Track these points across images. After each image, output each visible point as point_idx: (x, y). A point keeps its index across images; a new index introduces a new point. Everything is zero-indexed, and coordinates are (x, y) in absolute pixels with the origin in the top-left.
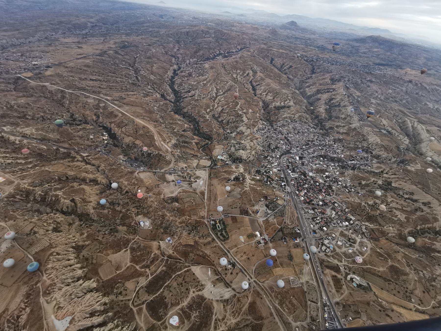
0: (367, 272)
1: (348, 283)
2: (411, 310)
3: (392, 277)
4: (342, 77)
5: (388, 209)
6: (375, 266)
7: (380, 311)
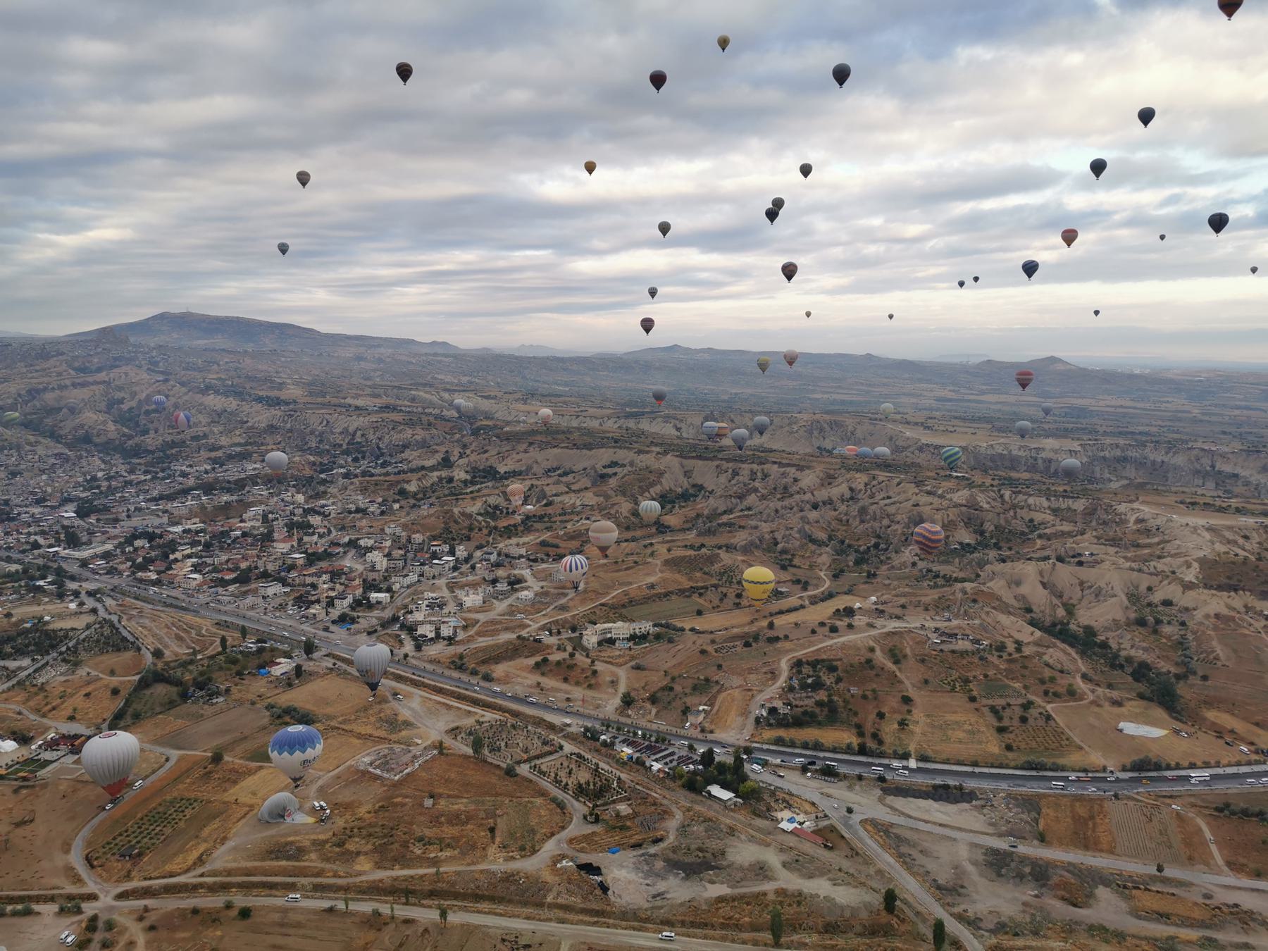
0: (624, 606)
1: (603, 654)
2: (802, 607)
3: (690, 579)
4: (116, 359)
5: (538, 501)
6: (631, 583)
7: (747, 645)
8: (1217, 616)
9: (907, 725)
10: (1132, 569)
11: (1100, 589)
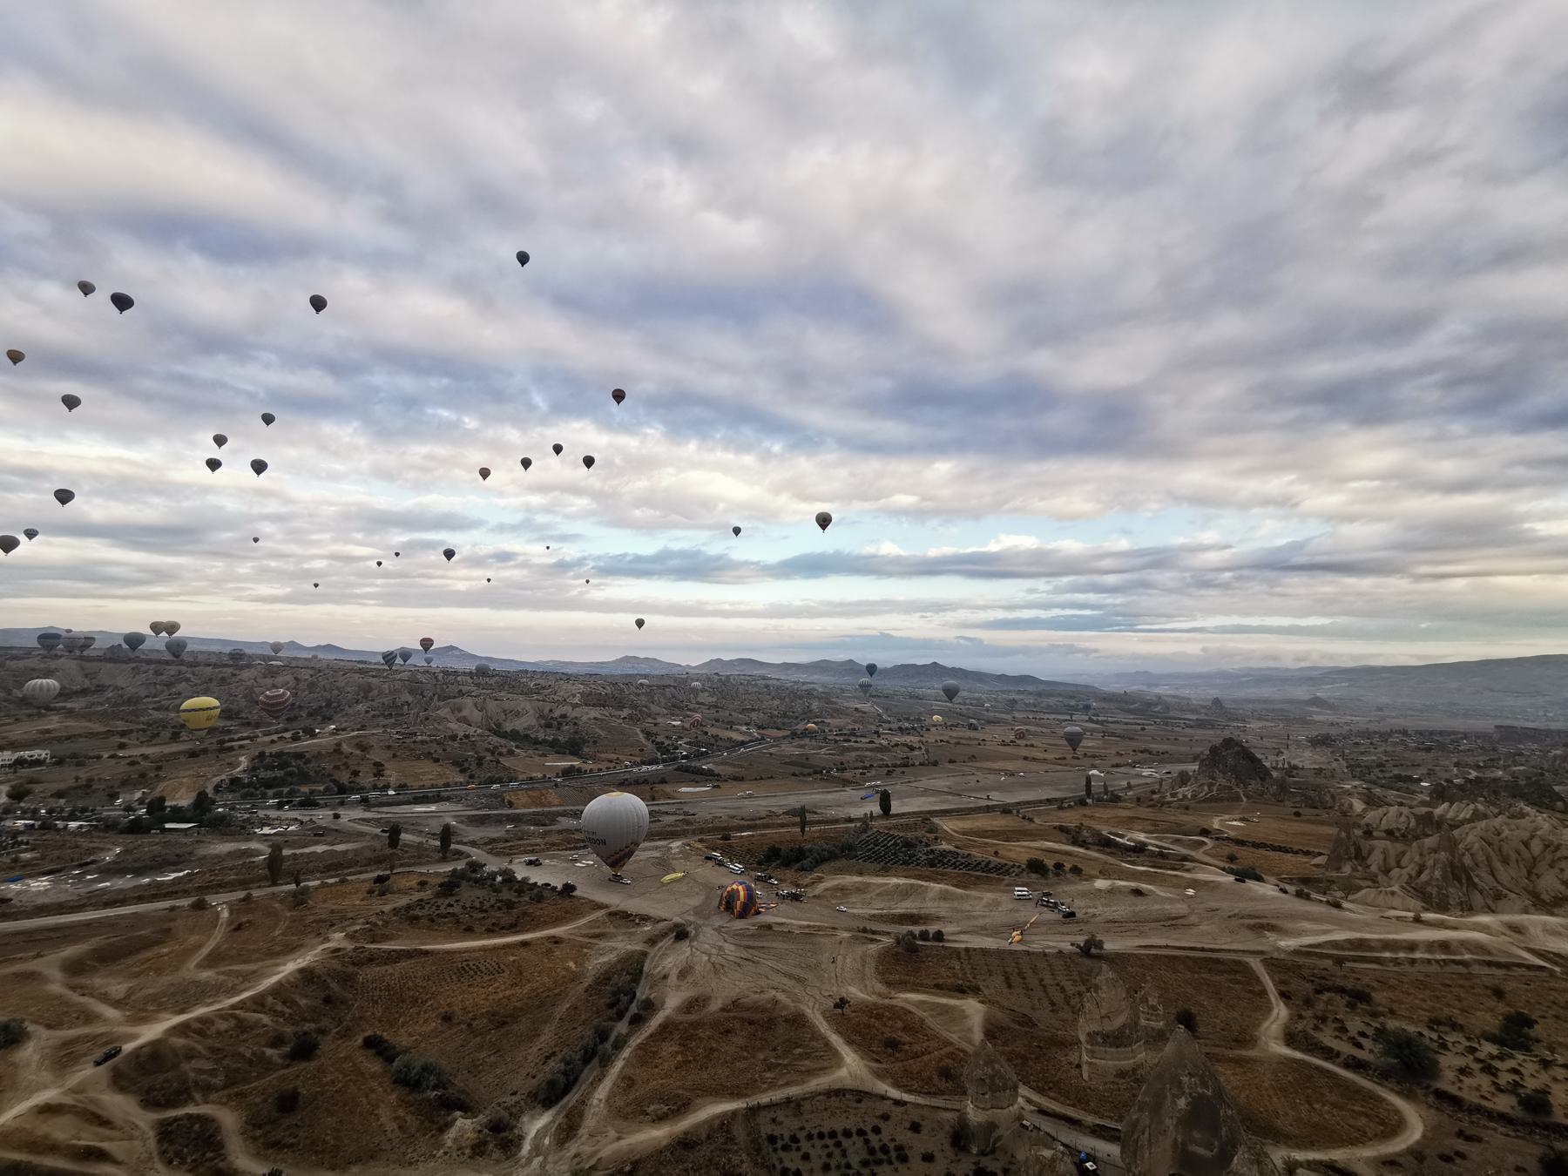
8: (595, 718)
9: (382, 776)
10: (538, 700)
11: (518, 712)
